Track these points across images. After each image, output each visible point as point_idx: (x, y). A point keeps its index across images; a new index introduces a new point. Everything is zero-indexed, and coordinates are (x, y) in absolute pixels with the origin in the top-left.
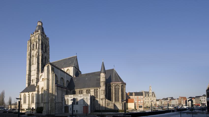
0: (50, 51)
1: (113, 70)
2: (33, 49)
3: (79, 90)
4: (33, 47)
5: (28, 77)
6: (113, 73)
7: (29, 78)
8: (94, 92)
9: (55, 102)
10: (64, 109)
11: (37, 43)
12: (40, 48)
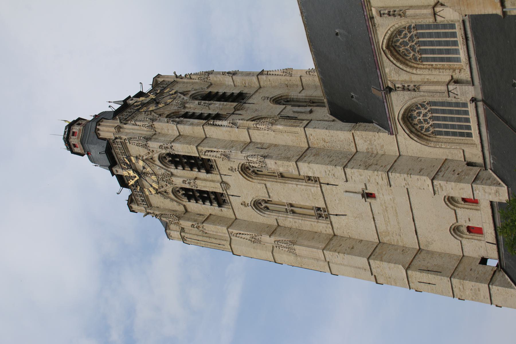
2: (219, 199)
4: (204, 196)
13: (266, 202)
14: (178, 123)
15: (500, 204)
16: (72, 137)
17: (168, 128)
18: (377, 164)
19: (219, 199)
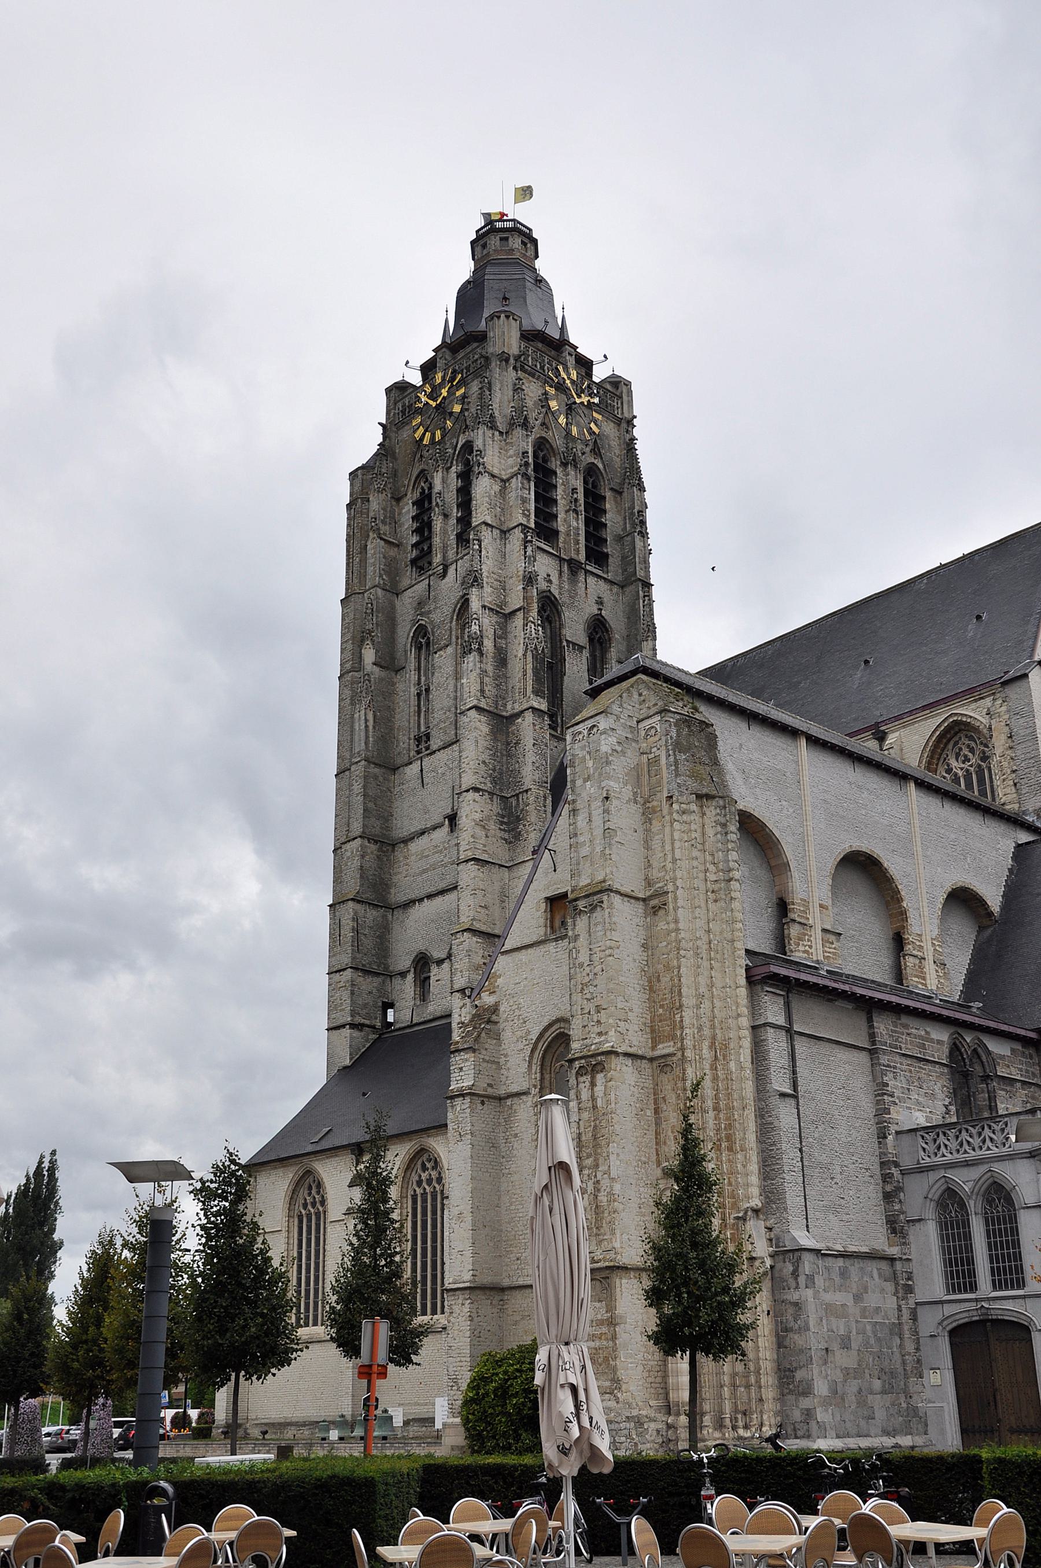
0: (653, 542)
2: (421, 562)
4: (424, 528)
5: (356, 931)
7: (368, 943)
10: (939, 1387)
13: (428, 644)
16: (498, 238)
18: (487, 836)
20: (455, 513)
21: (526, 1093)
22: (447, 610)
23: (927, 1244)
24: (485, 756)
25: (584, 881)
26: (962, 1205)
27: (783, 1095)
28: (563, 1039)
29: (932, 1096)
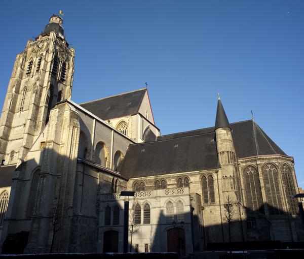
1: (249, 123)
2: (28, 74)
3: (153, 178)
4: (30, 68)
6: (252, 130)
8: (199, 186)
9: (71, 215)
10: (101, 241)
11: (40, 59)
12: (48, 69)
14: (52, 62)
15: (16, 166)
17: (50, 58)
19: (28, 74)
20: (37, 66)
21: (29, 180)
22: (32, 84)
23: (103, 215)
24: (34, 114)
25: (49, 140)
26: (110, 209)
27: (80, 185)
28: (39, 170)
29: (108, 188)
